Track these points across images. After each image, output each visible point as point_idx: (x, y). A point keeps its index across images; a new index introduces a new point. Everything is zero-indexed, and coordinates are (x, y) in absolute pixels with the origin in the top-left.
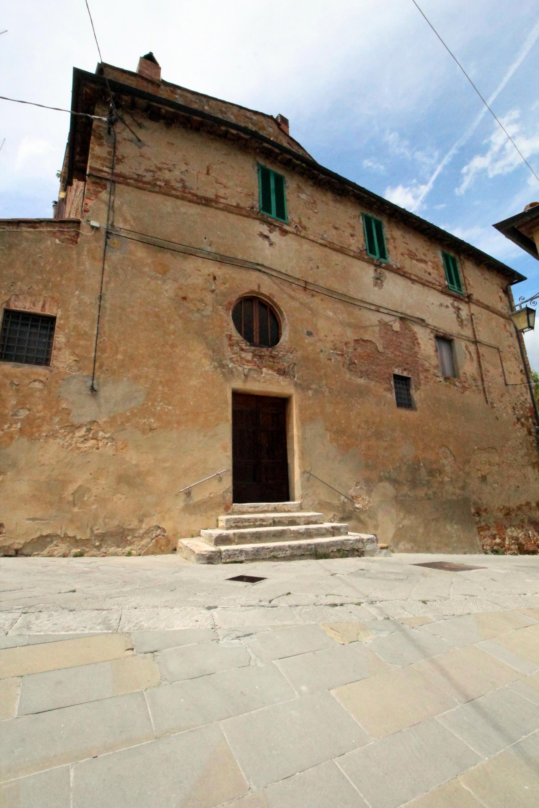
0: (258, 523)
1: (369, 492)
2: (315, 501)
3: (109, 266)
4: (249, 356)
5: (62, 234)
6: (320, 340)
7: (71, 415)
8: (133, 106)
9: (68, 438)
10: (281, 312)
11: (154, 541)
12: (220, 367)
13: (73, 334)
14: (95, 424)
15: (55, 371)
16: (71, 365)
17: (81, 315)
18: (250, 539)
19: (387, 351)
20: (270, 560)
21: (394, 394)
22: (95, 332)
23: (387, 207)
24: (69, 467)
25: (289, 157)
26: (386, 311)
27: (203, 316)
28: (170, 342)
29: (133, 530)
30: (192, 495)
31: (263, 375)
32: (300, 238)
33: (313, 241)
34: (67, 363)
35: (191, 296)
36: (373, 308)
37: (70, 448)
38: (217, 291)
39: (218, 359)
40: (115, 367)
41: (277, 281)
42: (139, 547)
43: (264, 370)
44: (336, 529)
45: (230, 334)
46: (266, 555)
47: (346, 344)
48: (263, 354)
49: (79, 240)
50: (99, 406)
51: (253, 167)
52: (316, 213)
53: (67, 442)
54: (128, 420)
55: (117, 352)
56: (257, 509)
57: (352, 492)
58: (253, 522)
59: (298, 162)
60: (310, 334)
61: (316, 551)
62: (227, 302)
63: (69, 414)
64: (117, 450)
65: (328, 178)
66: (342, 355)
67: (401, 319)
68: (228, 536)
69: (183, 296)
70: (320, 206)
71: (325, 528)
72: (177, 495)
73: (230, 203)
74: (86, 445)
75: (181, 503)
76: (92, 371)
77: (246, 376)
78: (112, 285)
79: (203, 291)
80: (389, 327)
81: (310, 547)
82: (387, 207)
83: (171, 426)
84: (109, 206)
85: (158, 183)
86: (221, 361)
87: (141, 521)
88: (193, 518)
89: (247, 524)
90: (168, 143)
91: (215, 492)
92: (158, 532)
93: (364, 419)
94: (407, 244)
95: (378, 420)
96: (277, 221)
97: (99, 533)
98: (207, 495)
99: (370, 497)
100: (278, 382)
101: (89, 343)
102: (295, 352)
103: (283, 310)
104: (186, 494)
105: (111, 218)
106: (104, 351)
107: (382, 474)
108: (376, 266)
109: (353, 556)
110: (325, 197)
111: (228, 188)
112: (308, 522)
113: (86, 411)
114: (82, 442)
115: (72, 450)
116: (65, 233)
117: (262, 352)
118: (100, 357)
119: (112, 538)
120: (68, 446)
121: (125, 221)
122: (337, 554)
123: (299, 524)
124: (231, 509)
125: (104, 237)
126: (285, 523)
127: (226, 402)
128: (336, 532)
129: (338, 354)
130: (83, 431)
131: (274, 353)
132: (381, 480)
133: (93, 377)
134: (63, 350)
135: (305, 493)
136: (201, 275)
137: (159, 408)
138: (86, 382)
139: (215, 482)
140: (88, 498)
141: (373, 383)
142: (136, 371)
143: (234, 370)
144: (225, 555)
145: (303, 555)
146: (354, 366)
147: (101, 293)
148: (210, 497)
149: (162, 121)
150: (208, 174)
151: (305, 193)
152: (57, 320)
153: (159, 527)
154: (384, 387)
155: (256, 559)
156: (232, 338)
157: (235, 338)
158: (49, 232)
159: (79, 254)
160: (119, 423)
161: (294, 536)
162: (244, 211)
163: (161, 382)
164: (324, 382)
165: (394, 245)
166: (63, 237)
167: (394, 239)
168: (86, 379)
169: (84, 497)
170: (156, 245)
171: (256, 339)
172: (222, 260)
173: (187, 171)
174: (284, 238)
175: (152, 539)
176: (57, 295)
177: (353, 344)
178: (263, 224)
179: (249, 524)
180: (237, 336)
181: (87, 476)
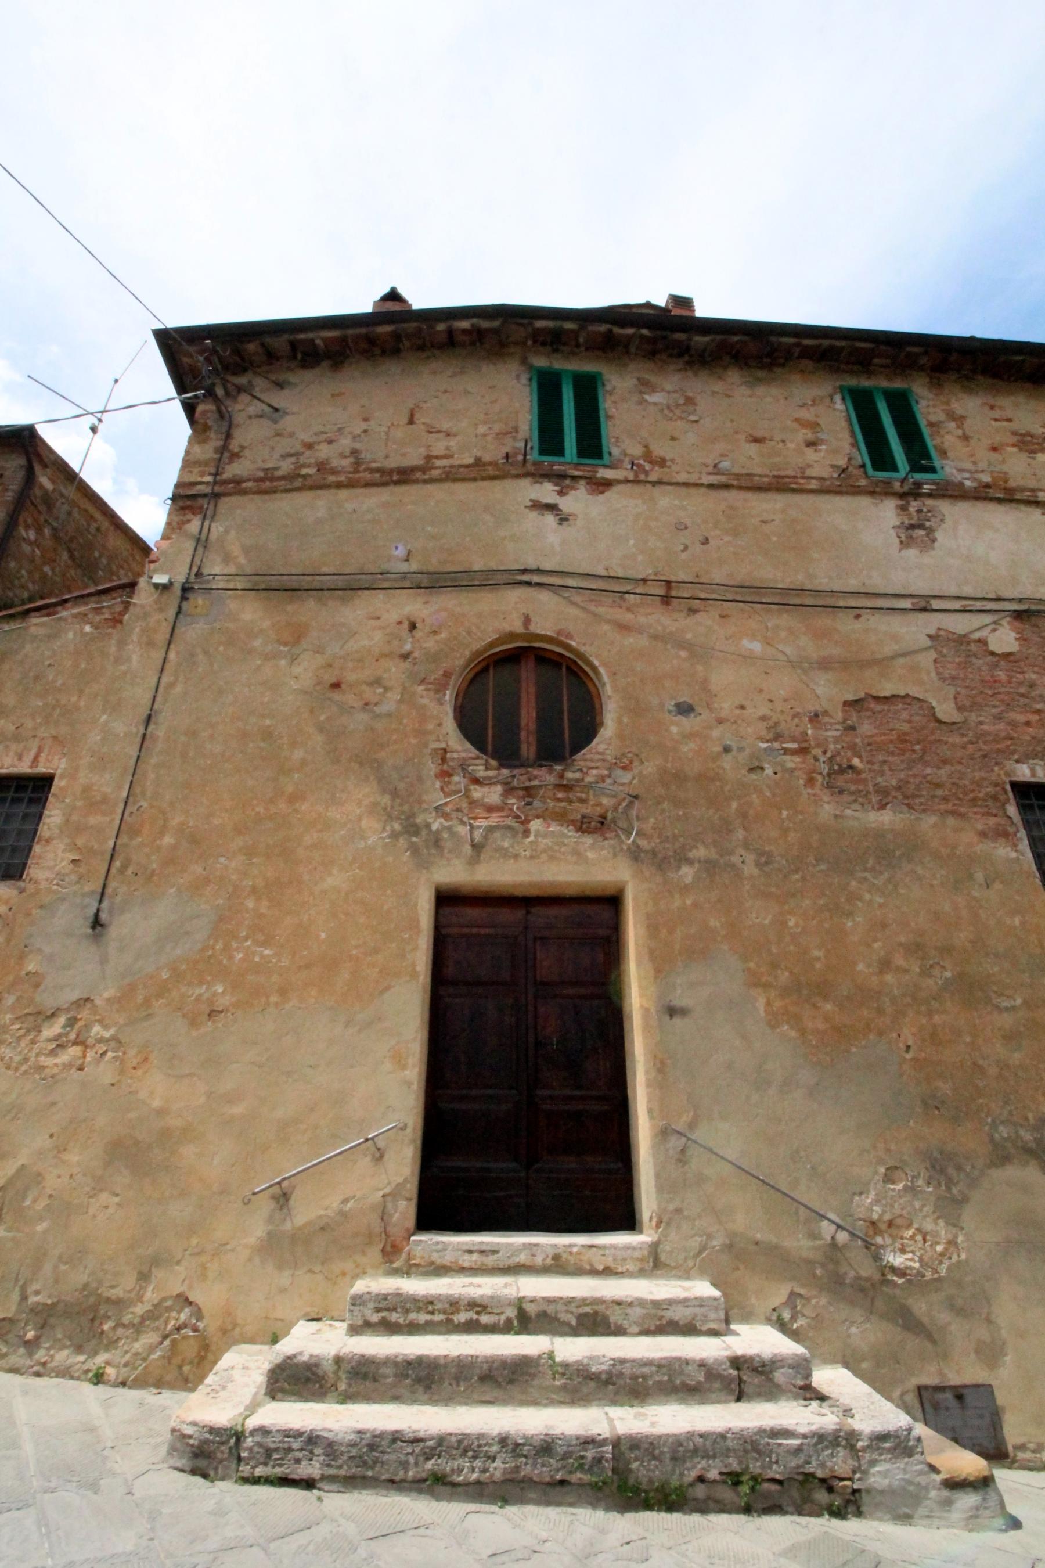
0: (462, 1317)
1: (951, 1207)
2: (710, 1237)
3: (178, 653)
4: (493, 795)
5: (97, 614)
6: (720, 721)
7: (42, 987)
8: (271, 356)
9: (23, 1044)
10: (594, 669)
11: (167, 1343)
12: (407, 832)
13: (79, 804)
14: (89, 1005)
15: (31, 888)
16: (63, 871)
17: (101, 763)
18: (394, 1386)
19: (973, 717)
20: (420, 1491)
21: (1024, 845)
22: (125, 794)
23: (916, 350)
24: (8, 1118)
25: (603, 328)
26: (957, 605)
27: (378, 716)
28: (290, 789)
29: (118, 1303)
30: (291, 1202)
31: (532, 838)
32: (649, 486)
33: (686, 485)
34: (57, 868)
35: (351, 677)
36: (907, 604)
37: (24, 1068)
38: (416, 654)
39: (403, 812)
40: (154, 866)
41: (577, 598)
42: (128, 1357)
43: (535, 825)
44: (755, 1370)
45: (443, 746)
46: (405, 1465)
47: (815, 717)
48: (535, 783)
49: (126, 617)
50: (104, 961)
51: (518, 377)
52: (696, 421)
53: (20, 1052)
54: (162, 990)
55: (162, 833)
56: (490, 1261)
57: (869, 1205)
58: (444, 1312)
59: (630, 331)
60: (685, 709)
61: (621, 1470)
62: (441, 672)
63: (37, 986)
64: (122, 1072)
65: (719, 337)
66: (803, 751)
67: (1019, 616)
68: (317, 1365)
69: (334, 680)
70: (703, 403)
71: (702, 1364)
72: (247, 1203)
73: (458, 462)
74: (58, 1061)
75: (257, 1230)
76: (102, 882)
77: (477, 847)
78: (179, 689)
79: (381, 660)
80: (973, 647)
81: (590, 1454)
82: (916, 350)
83: (263, 1000)
84: (198, 540)
85: (304, 471)
86: (412, 815)
87: (144, 1277)
88: (284, 1278)
89: (423, 1318)
90: (333, 395)
91: (359, 1194)
92: (183, 1317)
93: (902, 939)
94: (1009, 420)
95: (963, 937)
96: (577, 466)
97: (38, 1303)
98: (335, 1205)
99: (955, 1223)
100: (577, 853)
101: (108, 819)
102: (636, 763)
103: (596, 663)
104: (275, 1198)
105: (197, 561)
106: (135, 833)
107: (1004, 1131)
108: (902, 496)
109: (804, 1508)
110: (721, 383)
111: (455, 435)
112: (662, 1322)
113: (72, 971)
114: (53, 1053)
115: (25, 1072)
116: (104, 610)
117: (536, 777)
118: (126, 845)
119: (67, 1322)
120: (20, 1064)
121: (227, 559)
122: (726, 1493)
123: (619, 1331)
124: (404, 1256)
125: (178, 600)
126: (568, 1324)
127: (413, 924)
128: (752, 1381)
129: (786, 751)
130: (55, 1028)
131: (570, 775)
132: (1001, 1157)
133: (103, 894)
134: (55, 842)
135: (671, 1207)
136: (380, 628)
137: (241, 955)
138: (84, 907)
139: (365, 1163)
140: (35, 1201)
141: (930, 820)
142: (198, 869)
143: (445, 836)
144: (250, 1449)
145: (562, 1482)
146: (850, 775)
147: (151, 710)
148: (342, 1214)
149: (325, 364)
150: (411, 422)
151: (663, 390)
152: (56, 781)
153: (187, 1299)
154: (980, 826)
155: (364, 1478)
156: (448, 755)
157: (455, 755)
158: (75, 616)
159: (121, 644)
160: (140, 999)
161: (564, 1387)
162: (490, 468)
163: (254, 890)
164: (740, 834)
165: (960, 432)
166: (98, 618)
167: (960, 420)
168: (87, 900)
169: (24, 1198)
170: (279, 587)
171: (528, 748)
172: (433, 582)
173: (365, 431)
174: (601, 498)
175: (165, 1337)
176: (64, 730)
177: (840, 716)
178: (541, 483)
179: (428, 1317)
180: (460, 747)
181: (42, 1141)
